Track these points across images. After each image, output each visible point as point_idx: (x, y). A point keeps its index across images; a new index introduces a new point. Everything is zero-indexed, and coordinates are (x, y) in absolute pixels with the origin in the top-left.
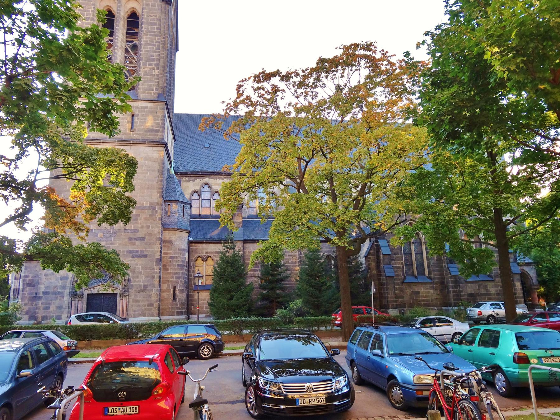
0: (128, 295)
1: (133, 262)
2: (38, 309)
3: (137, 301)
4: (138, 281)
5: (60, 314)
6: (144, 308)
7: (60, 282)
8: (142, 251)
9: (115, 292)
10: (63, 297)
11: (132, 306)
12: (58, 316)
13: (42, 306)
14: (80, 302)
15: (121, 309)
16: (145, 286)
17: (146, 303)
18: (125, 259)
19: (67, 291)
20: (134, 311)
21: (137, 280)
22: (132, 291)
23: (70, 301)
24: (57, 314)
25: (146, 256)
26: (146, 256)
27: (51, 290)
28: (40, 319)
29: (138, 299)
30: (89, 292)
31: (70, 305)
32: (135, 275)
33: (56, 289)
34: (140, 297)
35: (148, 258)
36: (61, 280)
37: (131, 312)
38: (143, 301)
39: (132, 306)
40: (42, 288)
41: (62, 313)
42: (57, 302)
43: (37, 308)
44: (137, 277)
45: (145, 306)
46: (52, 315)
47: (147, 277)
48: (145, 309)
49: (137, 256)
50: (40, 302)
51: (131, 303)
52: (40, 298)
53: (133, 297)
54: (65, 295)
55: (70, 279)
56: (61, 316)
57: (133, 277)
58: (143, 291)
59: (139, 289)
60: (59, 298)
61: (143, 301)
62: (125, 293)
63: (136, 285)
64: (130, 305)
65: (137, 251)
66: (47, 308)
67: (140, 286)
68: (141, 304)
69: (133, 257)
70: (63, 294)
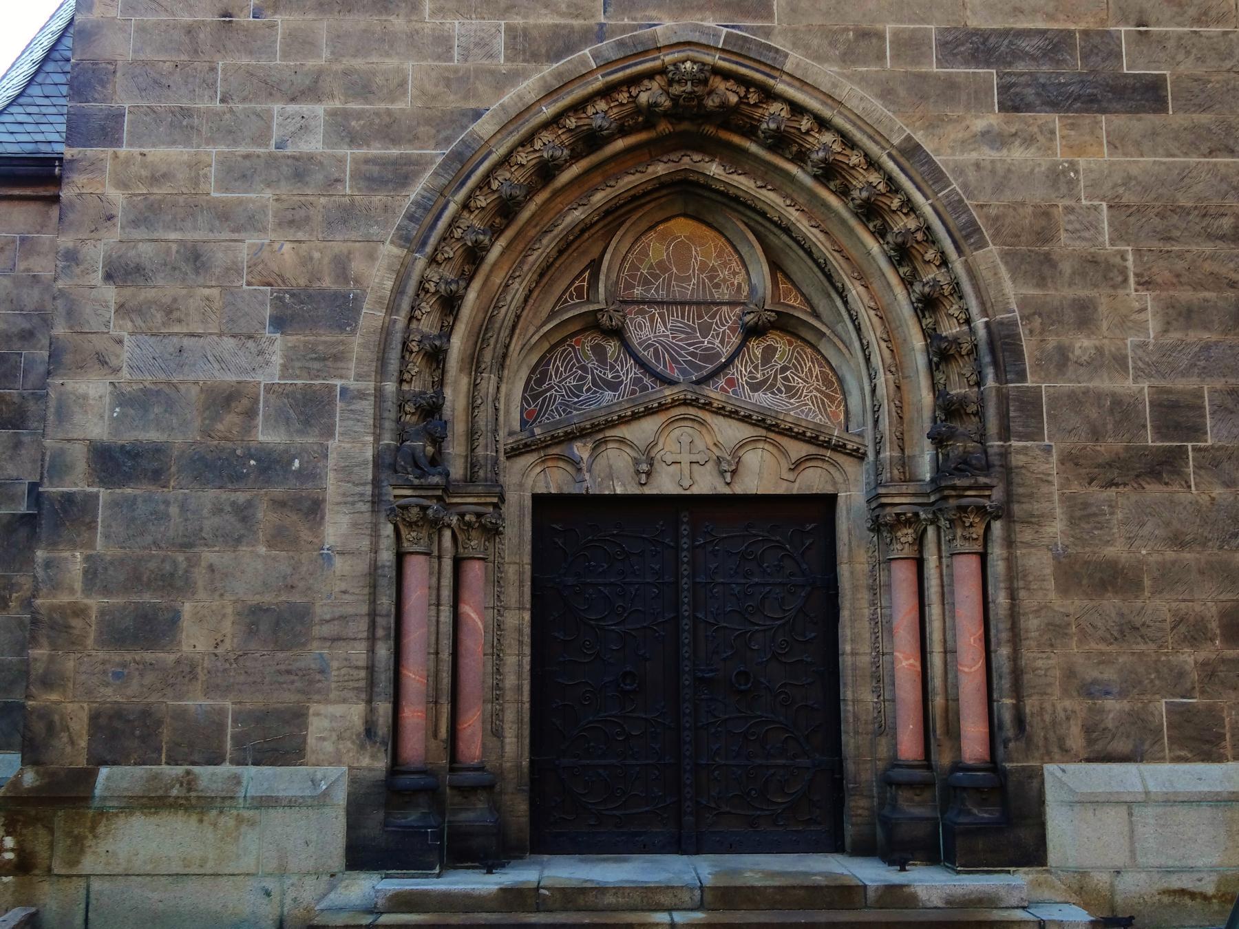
0: (1004, 512)
1: (1018, 154)
2: (58, 628)
3: (1114, 579)
4: (1098, 362)
5: (287, 698)
6: (1188, 658)
7: (277, 346)
8: (1100, 45)
9: (813, 481)
10: (314, 510)
11: (1057, 630)
12: (261, 717)
13: (94, 603)
14: (475, 572)
15: (905, 662)
16: (1177, 416)
17: (1208, 602)
18: (932, 126)
19: (352, 445)
20: (1089, 690)
21: (1083, 344)
22: (1041, 460)
23: (387, 556)
24: (254, 702)
25: (1150, 95)
26: (1150, 95)
27: (179, 434)
28: (73, 748)
29: (1116, 551)
30: (556, 480)
31: (386, 602)
32: (1063, 293)
33: (229, 422)
34: (1132, 528)
35: (1175, 118)
36: (280, 323)
37: (1054, 704)
38: (1167, 578)
39: (1057, 630)
40: (90, 408)
41: (311, 683)
42: (253, 569)
43: (37, 626)
44: (1084, 315)
45: (1195, 633)
46: (196, 702)
47: (1187, 316)
48: (1209, 671)
49: (1058, 99)
50: (75, 562)
51: (1046, 598)
52: (71, 514)
53: (1057, 528)
54: (332, 487)
55: (371, 316)
56: (298, 717)
57: (1032, 311)
58: (1163, 466)
59: (1112, 446)
60: (265, 516)
61: (1167, 578)
62: (966, 489)
63: (1075, 401)
64: (1032, 624)
65: (1056, 45)
66: (151, 629)
67: (1123, 409)
68: (1158, 607)
69: (1012, 103)
70: (310, 475)
